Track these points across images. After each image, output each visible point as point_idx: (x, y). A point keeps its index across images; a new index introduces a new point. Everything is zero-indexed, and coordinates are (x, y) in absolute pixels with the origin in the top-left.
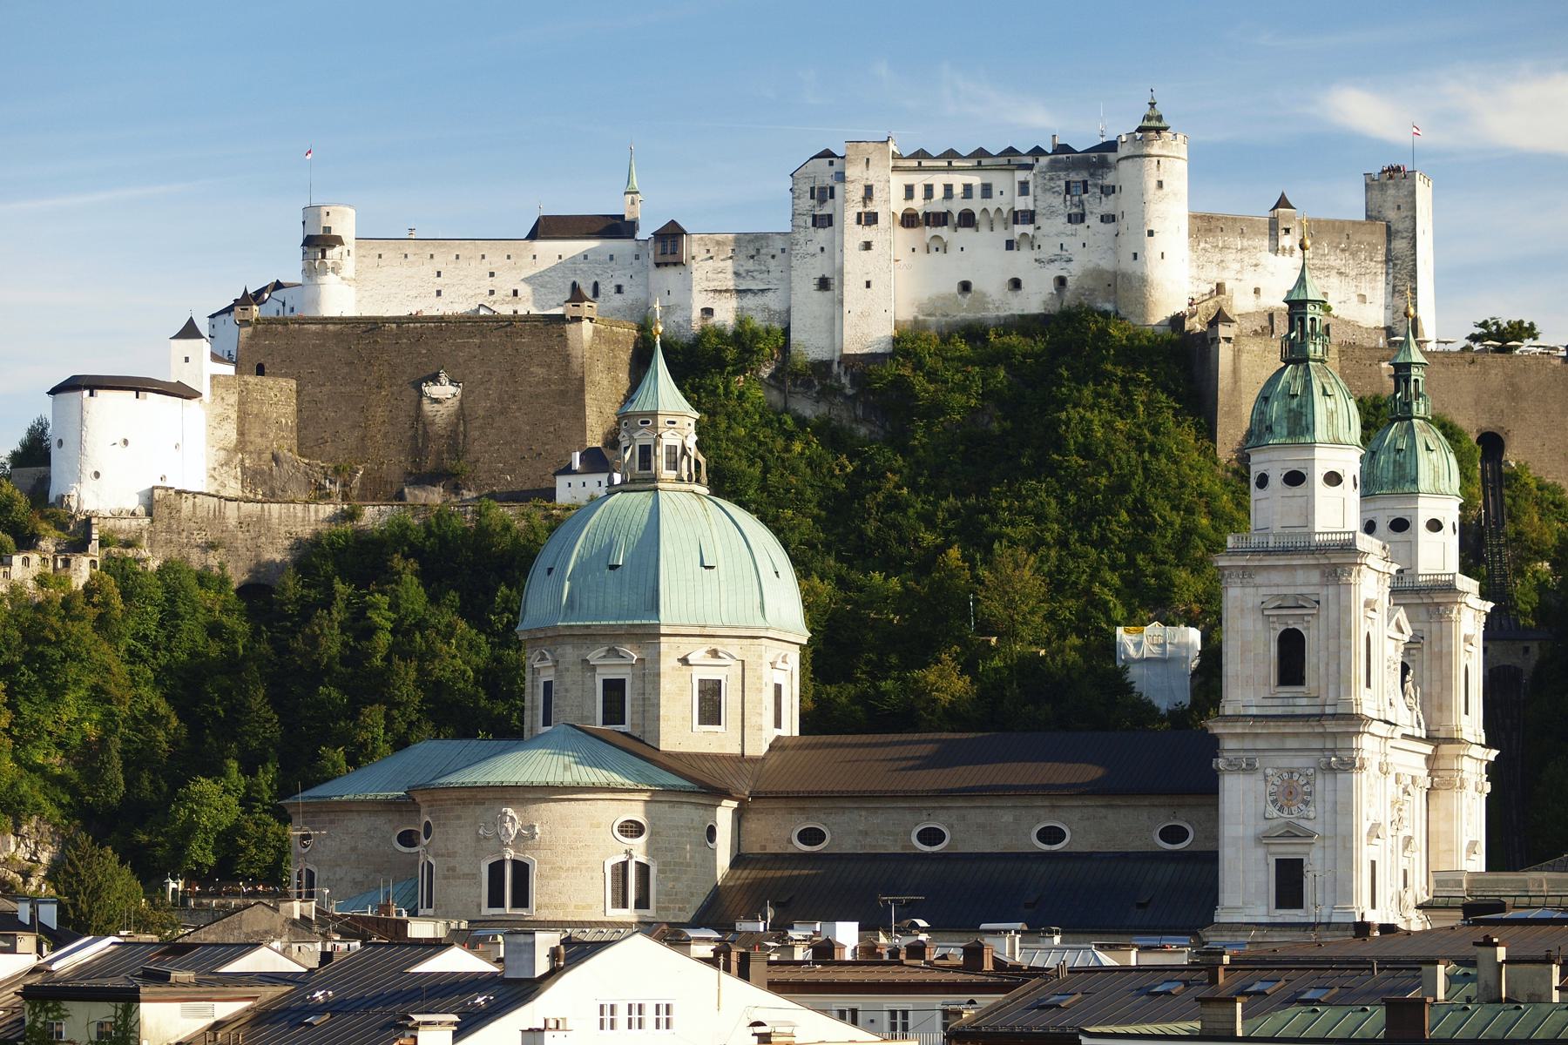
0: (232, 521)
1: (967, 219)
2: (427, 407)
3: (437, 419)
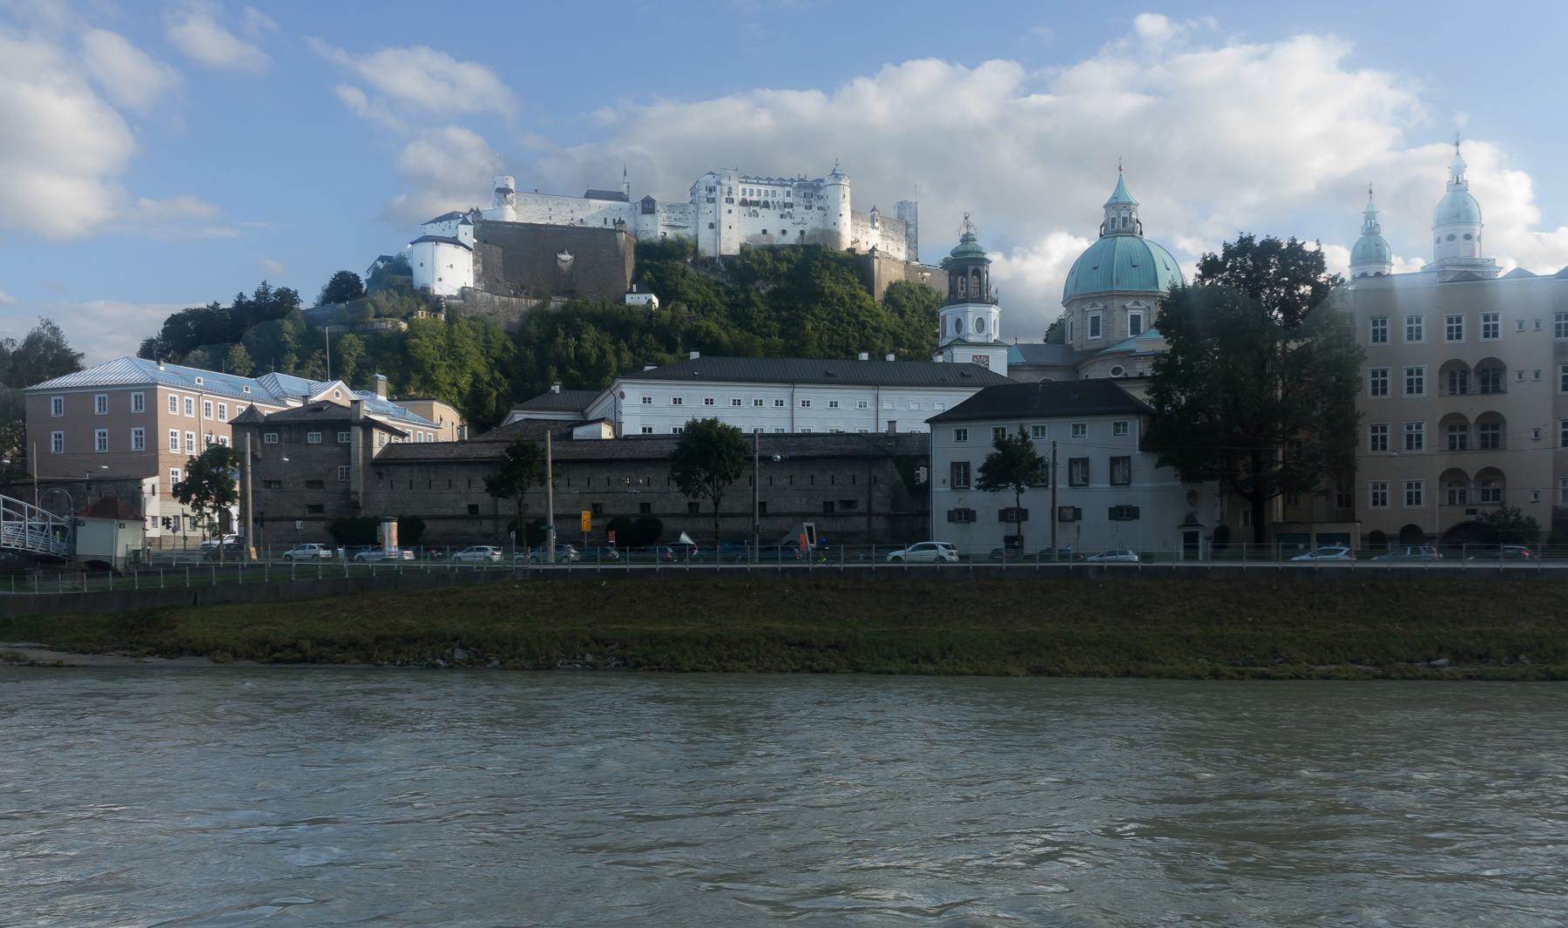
1: (766, 205)
2: (559, 263)
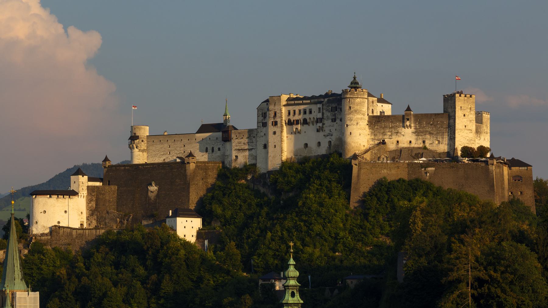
0: (74, 236)
2: (150, 194)
3: (152, 198)
